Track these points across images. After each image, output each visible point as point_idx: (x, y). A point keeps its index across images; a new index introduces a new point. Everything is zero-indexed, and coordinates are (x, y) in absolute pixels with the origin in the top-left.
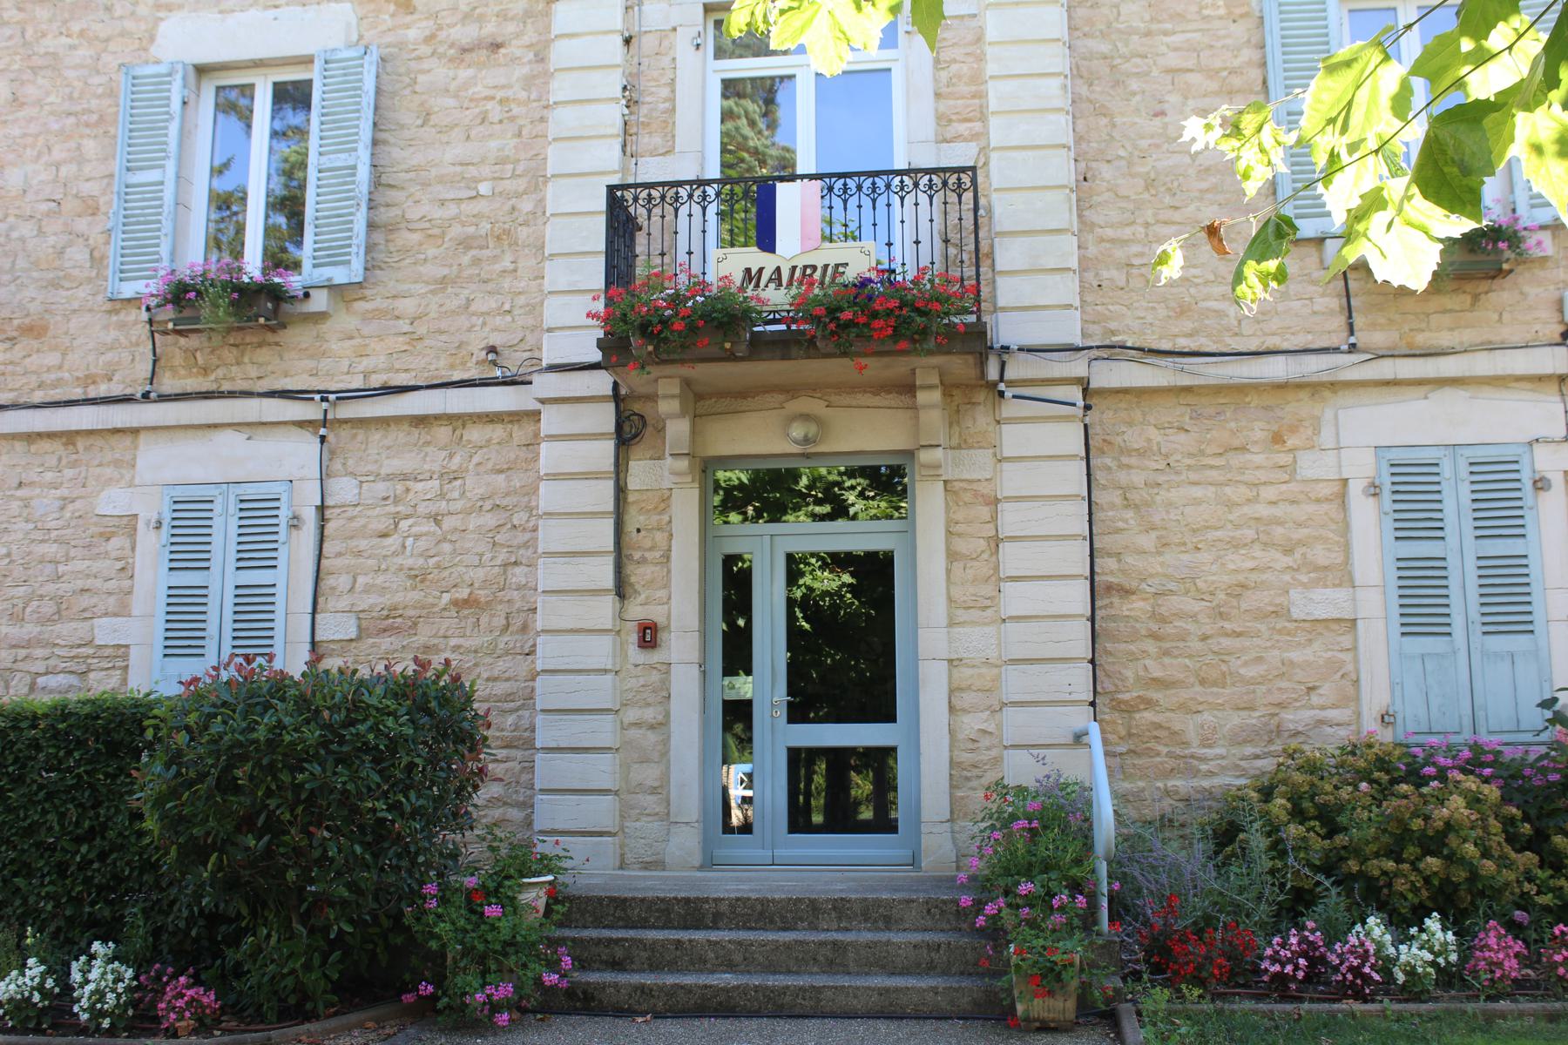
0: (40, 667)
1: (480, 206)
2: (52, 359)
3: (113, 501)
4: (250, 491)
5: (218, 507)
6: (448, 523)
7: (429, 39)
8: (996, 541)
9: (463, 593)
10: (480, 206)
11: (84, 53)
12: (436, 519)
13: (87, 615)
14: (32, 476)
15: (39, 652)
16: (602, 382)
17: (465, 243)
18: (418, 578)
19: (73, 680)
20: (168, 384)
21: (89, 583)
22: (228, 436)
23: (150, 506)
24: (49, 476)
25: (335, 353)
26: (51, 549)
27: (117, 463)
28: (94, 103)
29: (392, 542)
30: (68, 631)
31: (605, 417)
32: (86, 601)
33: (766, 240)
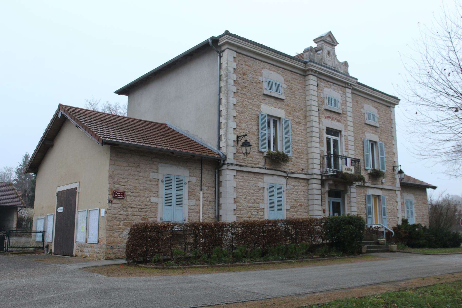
0: (252, 211)
1: (299, 147)
2: (251, 159)
3: (261, 184)
4: (279, 185)
5: (275, 187)
6: (299, 193)
7: (293, 120)
8: (350, 202)
9: (300, 203)
10: (299, 147)
11: (251, 107)
12: (297, 192)
13: (259, 203)
14: (249, 178)
15: (252, 208)
16: (320, 177)
17: (299, 152)
18: (295, 200)
19: (256, 213)
20: (266, 167)
21: (258, 197)
22: (275, 177)
23: (266, 187)
24: (252, 179)
25: (289, 167)
26: (253, 191)
27: (261, 178)
28: (253, 116)
29: (293, 195)
30: (256, 205)
31: (319, 182)
32: (258, 200)
33: (346, 165)
